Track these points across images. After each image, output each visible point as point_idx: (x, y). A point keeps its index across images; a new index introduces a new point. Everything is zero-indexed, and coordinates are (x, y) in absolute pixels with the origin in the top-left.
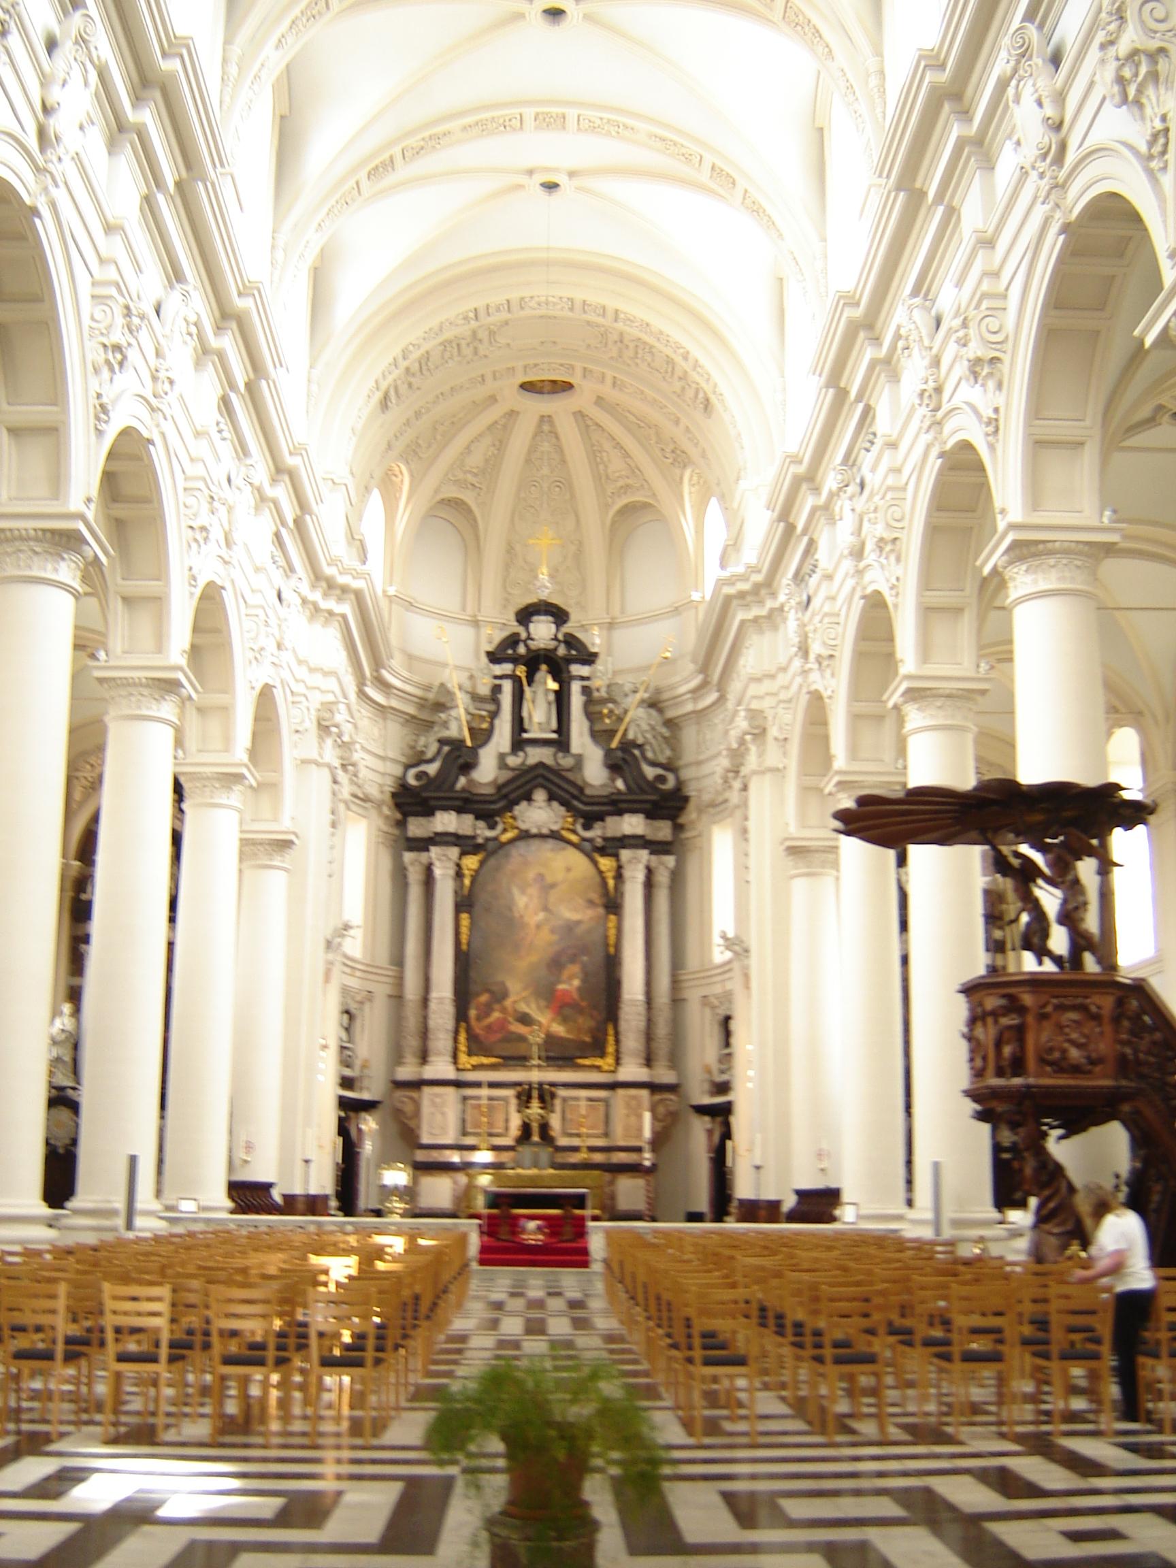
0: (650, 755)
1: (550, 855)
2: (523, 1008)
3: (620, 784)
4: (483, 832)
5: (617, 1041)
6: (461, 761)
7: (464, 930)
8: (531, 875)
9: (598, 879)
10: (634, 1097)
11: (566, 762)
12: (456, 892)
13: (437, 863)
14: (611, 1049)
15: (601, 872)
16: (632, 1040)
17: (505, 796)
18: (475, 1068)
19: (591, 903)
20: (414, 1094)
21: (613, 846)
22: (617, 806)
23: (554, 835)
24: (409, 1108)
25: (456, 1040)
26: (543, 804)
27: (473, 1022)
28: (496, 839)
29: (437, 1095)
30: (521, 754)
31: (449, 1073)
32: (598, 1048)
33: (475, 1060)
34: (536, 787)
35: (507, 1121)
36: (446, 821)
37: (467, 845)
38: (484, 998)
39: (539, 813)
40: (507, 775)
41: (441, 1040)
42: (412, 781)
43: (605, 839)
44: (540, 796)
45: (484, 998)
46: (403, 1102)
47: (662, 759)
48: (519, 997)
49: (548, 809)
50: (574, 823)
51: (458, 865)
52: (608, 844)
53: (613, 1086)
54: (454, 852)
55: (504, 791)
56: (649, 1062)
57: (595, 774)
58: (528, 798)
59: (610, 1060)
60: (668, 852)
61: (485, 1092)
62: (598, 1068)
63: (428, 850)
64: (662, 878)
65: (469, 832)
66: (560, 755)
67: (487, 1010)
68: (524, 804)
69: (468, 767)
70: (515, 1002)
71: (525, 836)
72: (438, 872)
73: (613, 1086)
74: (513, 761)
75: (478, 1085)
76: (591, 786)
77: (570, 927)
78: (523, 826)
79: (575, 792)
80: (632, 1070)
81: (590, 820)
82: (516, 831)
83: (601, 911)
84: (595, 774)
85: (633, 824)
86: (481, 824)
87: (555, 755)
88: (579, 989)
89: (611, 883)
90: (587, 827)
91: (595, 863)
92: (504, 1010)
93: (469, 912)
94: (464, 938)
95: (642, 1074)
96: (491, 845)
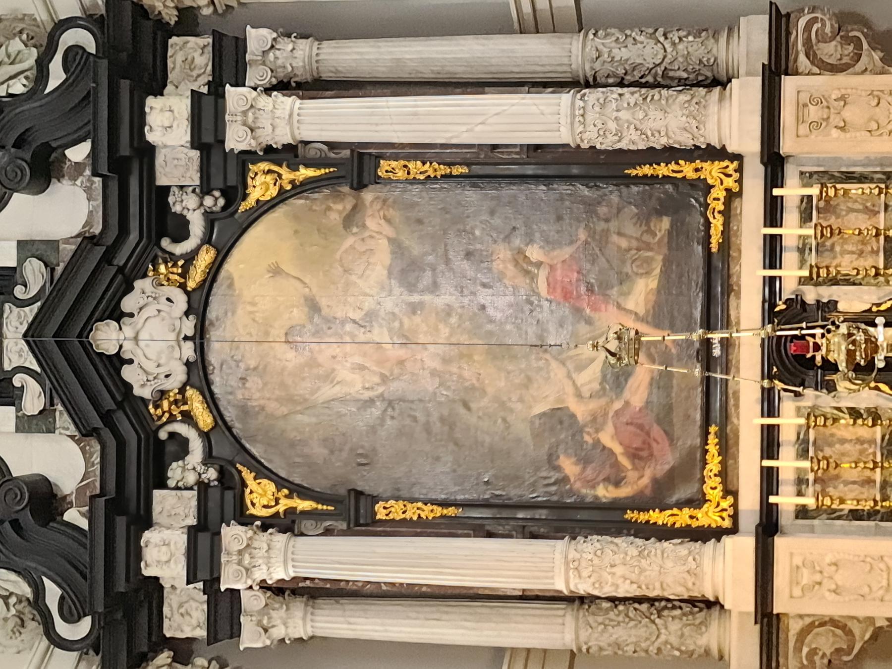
0: (18, 87)
1: (241, 315)
2: (590, 376)
3: (78, 153)
4: (189, 469)
5: (671, 154)
6: (27, 519)
7: (412, 512)
8: (289, 357)
9: (298, 202)
10: (801, 107)
11: (35, 275)
12: (328, 532)
13: (259, 575)
14: (688, 170)
15: (282, 197)
16: (666, 120)
17: (106, 417)
18: (730, 491)
19: (350, 220)
20: (795, 627)
21: (223, 171)
22: (127, 162)
23: (199, 305)
24: (825, 643)
25: (665, 533)
26: (128, 331)
27: (624, 492)
28: (206, 436)
29: (794, 581)
30: (17, 380)
31: (741, 548)
32: (680, 201)
33: (713, 489)
34: (87, 347)
35: (855, 413)
36: (163, 552)
37: (221, 504)
38: (569, 467)
39: (148, 338)
40: (62, 419)
41: (665, 568)
42: (83, 628)
43: (205, 189)
44: (107, 337)
45: (569, 467)
46: (813, 652)
47: (31, 56)
48: (570, 382)
49: (139, 319)
50: (172, 258)
51: (266, 525)
52: (217, 180)
53: (774, 164)
54: (233, 535)
55: (97, 423)
56: (717, 82)
57: (65, 211)
58: (118, 361)
59: (712, 171)
60: (240, 44)
61: (787, 463)
62: (732, 196)
63: (234, 594)
64: (297, 56)
65: (192, 497)
66: (19, 291)
67: (591, 454)
68: (128, 373)
69: (44, 498)
70: (579, 395)
71: (199, 372)
72: (279, 573)
73: (774, 164)
74: (34, 399)
75: (769, 481)
76: (88, 223)
77: (407, 270)
78: (180, 375)
79: (100, 251)
80: (734, 121)
81: (165, 223)
82: (190, 392)
83: (368, 195)
84: (65, 211)
85: (167, 121)
86: (175, 472)
87: (22, 304)
88: (549, 243)
89: (305, 173)
90: (181, 232)
91: (264, 208)
92: (597, 421)
93: (375, 499)
94: (429, 512)
95: (747, 92)
96: (223, 449)
